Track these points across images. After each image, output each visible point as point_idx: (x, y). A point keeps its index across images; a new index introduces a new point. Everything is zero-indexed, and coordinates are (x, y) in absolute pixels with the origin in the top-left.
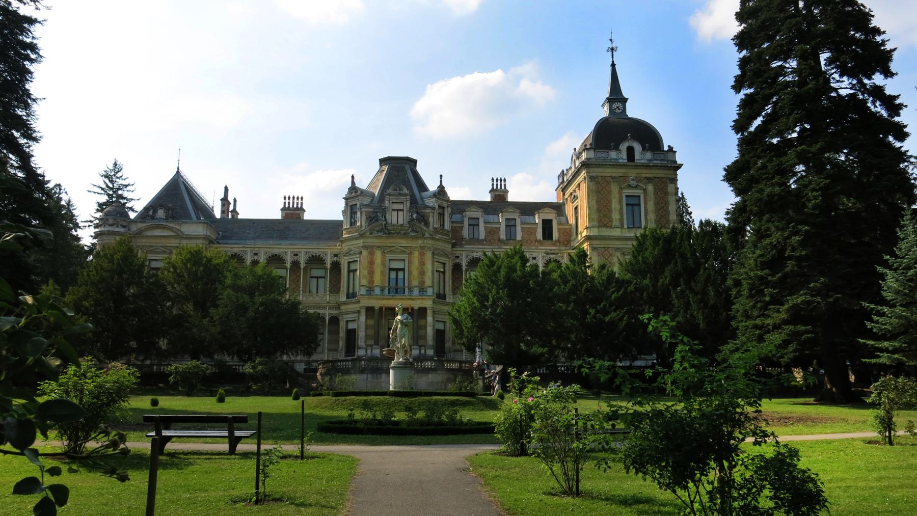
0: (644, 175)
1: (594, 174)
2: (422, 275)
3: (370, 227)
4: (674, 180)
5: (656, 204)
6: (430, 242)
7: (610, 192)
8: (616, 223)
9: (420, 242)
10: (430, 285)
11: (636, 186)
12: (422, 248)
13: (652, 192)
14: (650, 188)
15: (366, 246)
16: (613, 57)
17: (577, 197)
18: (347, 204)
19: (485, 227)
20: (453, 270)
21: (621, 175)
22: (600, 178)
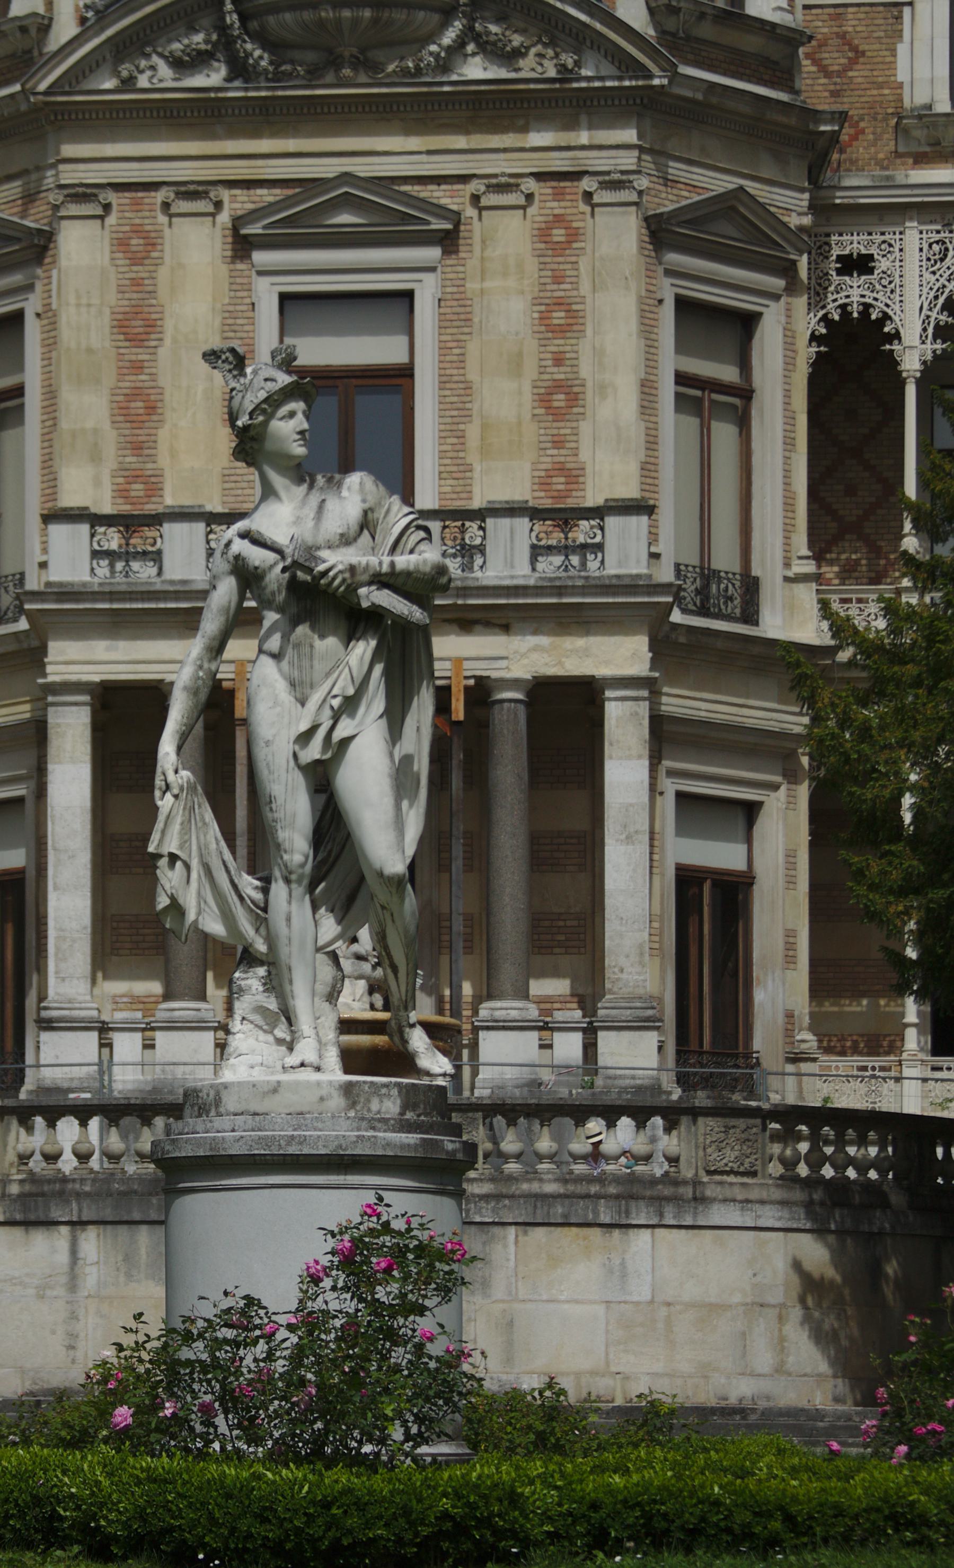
2: (558, 415)
10: (629, 490)
20: (819, 367)
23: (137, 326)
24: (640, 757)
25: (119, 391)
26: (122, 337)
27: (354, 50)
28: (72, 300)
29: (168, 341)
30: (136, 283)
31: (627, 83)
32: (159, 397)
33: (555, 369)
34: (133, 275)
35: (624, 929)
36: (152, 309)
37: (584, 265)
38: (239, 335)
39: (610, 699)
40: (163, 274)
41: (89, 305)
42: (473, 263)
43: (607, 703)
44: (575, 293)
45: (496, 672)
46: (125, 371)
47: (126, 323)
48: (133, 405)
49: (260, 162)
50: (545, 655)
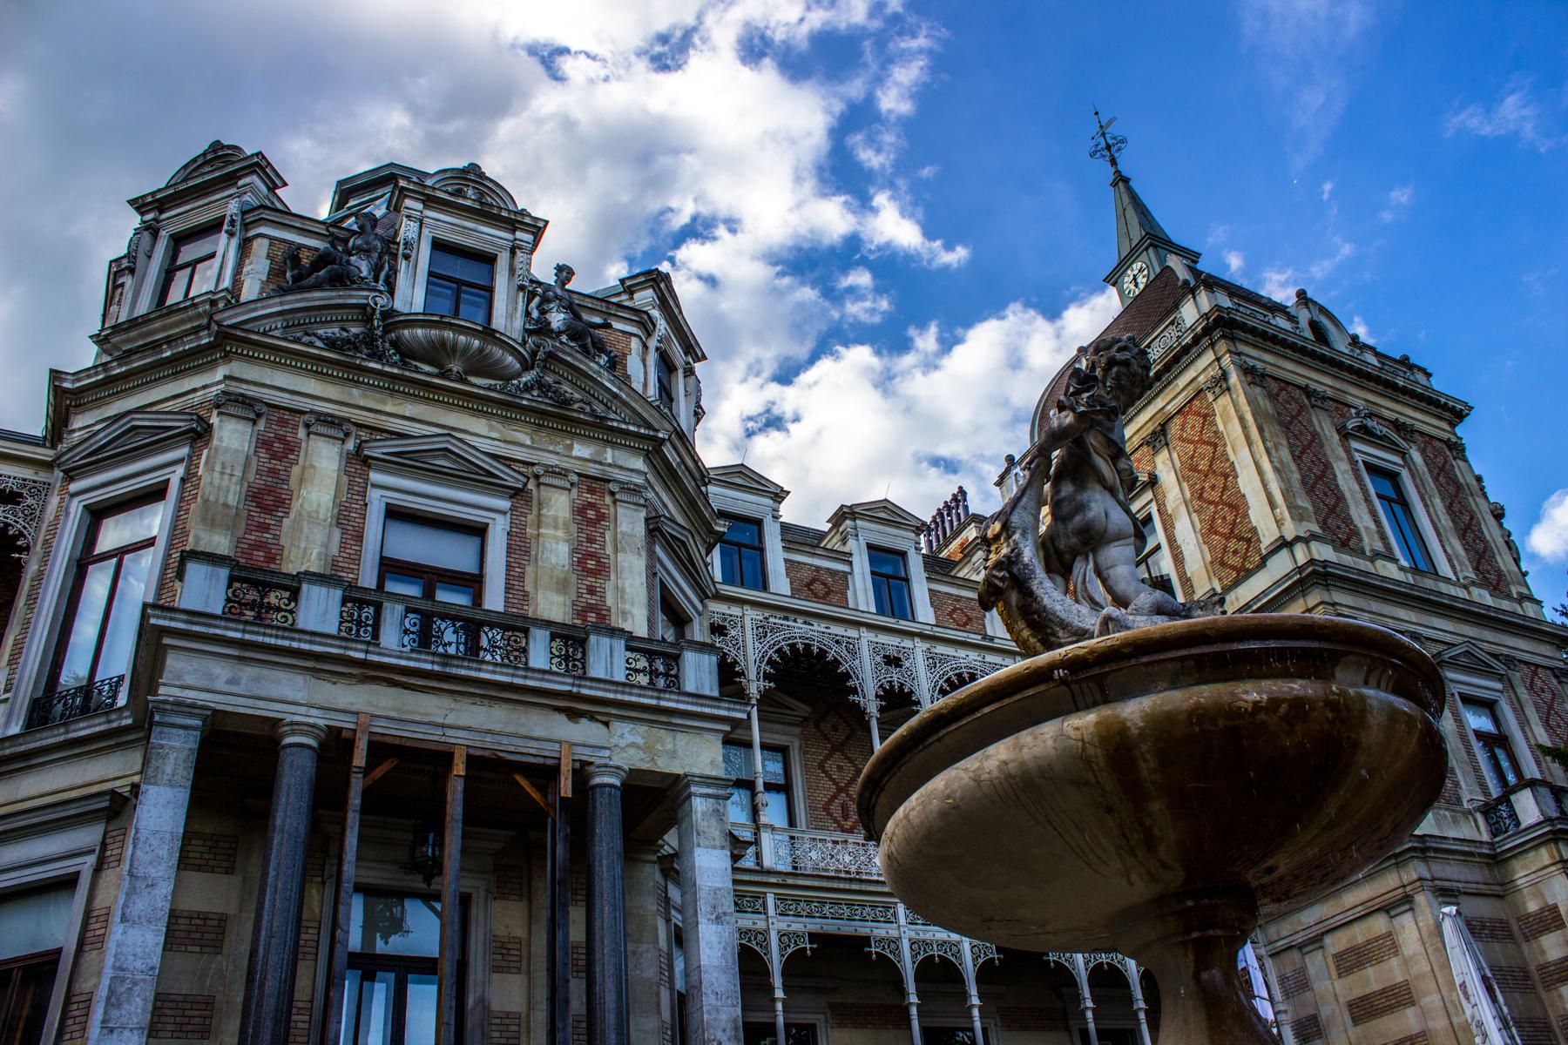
0: (1386, 413)
1: (1259, 365)
3: (293, 301)
4: (1457, 449)
5: (1449, 508)
6: (639, 463)
7: (1315, 435)
8: (1370, 542)
9: (581, 450)
11: (1380, 438)
12: (595, 483)
13: (1426, 469)
14: (1416, 456)
15: (246, 402)
16: (1113, 162)
17: (1153, 481)
18: (152, 229)
19: (786, 561)
21: (1329, 392)
22: (1274, 386)
23: (269, 500)
24: (723, 848)
25: (245, 541)
26: (254, 504)
27: (461, 370)
28: (218, 468)
29: (292, 515)
30: (273, 472)
31: (642, 431)
32: (278, 552)
33: (589, 597)
34: (272, 466)
35: (719, 1003)
36: (283, 491)
37: (608, 536)
38: (351, 523)
39: (696, 795)
40: (296, 470)
41: (231, 475)
42: (531, 518)
43: (693, 798)
44: (602, 552)
45: (598, 758)
46: (253, 528)
47: (260, 496)
48: (255, 553)
49: (383, 418)
50: (641, 752)
